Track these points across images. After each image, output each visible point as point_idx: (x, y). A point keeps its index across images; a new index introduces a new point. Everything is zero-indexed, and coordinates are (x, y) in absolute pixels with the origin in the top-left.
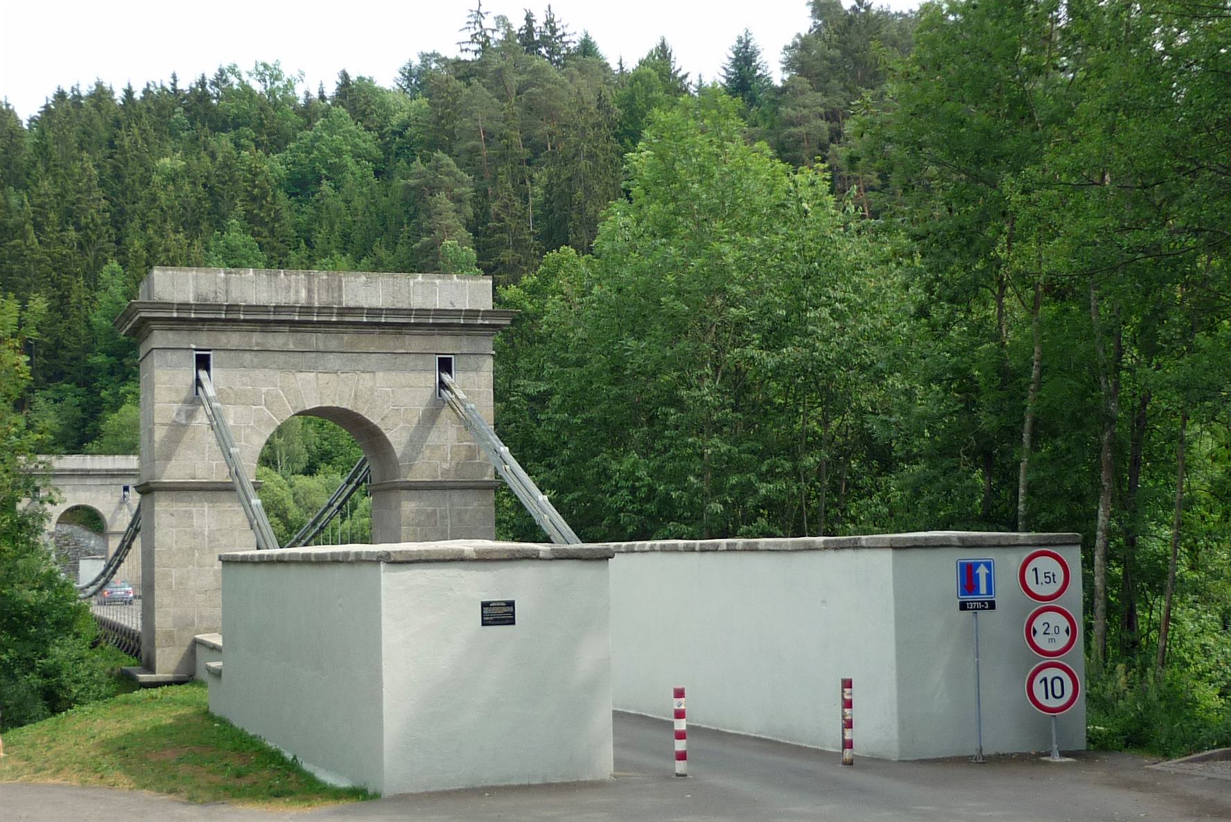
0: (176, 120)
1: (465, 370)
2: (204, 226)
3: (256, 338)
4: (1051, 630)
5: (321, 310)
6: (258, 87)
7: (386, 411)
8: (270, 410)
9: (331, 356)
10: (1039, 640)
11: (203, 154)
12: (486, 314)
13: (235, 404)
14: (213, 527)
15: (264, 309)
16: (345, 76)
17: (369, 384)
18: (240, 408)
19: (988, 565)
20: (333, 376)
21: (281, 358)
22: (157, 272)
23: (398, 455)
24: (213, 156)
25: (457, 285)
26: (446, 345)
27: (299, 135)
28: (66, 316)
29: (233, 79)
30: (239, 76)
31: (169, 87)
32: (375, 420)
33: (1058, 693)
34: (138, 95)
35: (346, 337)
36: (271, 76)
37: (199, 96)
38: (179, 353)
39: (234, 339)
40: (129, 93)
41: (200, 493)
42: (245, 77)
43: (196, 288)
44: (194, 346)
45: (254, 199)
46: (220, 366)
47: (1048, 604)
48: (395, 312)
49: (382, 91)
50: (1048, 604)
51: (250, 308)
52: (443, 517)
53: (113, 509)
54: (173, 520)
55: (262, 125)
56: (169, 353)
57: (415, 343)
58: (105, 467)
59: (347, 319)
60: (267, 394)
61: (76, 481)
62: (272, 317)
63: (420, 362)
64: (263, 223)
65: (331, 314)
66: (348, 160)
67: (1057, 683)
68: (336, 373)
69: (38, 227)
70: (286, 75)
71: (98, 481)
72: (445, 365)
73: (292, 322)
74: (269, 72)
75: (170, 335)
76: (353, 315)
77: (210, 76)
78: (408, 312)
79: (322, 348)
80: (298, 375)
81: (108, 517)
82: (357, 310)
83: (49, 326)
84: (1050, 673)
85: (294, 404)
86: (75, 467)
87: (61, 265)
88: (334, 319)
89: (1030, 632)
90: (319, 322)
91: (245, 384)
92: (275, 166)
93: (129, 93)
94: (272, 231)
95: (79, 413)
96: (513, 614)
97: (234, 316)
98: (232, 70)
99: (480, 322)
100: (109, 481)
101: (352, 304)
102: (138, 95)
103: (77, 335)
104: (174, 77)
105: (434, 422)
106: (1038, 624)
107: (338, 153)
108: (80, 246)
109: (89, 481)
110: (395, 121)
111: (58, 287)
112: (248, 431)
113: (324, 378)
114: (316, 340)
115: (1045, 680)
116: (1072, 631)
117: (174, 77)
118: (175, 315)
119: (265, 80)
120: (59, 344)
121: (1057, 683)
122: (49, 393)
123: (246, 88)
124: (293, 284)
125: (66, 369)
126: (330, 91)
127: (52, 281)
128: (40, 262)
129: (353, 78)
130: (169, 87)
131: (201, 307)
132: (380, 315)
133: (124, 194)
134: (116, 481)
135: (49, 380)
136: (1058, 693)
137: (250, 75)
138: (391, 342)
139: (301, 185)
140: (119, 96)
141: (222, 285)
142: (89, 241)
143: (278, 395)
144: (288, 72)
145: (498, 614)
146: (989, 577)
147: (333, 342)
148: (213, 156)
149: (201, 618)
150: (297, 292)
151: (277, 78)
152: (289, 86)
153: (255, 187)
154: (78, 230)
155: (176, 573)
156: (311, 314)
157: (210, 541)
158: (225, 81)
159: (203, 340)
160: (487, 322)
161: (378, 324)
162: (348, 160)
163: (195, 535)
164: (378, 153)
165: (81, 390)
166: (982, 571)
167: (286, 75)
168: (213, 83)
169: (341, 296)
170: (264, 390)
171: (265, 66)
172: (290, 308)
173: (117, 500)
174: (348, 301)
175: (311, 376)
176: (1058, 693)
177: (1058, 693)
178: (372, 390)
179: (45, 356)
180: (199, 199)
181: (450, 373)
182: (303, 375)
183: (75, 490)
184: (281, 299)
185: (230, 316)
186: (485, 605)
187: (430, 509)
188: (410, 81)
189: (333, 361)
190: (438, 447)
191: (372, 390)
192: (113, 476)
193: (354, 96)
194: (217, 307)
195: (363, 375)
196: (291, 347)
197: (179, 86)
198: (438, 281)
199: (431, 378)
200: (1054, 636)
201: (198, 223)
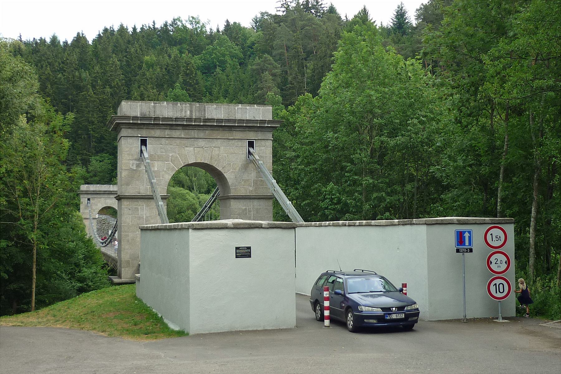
0: (154, 41)
1: (260, 146)
2: (165, 86)
3: (167, 132)
4: (498, 262)
5: (196, 120)
6: (189, 26)
9: (200, 140)
10: (493, 266)
11: (165, 55)
12: (269, 122)
14: (148, 215)
15: (170, 119)
16: (227, 21)
17: (217, 152)
18: (160, 163)
19: (469, 232)
20: (201, 149)
21: (178, 141)
22: (123, 103)
23: (230, 184)
24: (170, 56)
25: (256, 109)
26: (252, 136)
27: (207, 47)
28: (105, 125)
29: (179, 23)
30: (181, 21)
31: (152, 27)
32: (220, 169)
33: (501, 290)
34: (138, 30)
35: (207, 132)
37: (165, 29)
38: (133, 138)
39: (157, 132)
40: (135, 29)
41: (142, 200)
42: (184, 22)
43: (141, 110)
45: (187, 75)
46: (151, 144)
47: (497, 250)
48: (229, 121)
49: (244, 28)
50: (497, 250)
51: (164, 119)
52: (250, 211)
54: (130, 212)
56: (129, 138)
57: (238, 134)
59: (207, 124)
60: (172, 156)
62: (174, 123)
63: (240, 143)
64: (191, 85)
65: (200, 122)
66: (228, 58)
67: (501, 286)
69: (93, 87)
72: (251, 144)
73: (183, 125)
74: (194, 20)
75: (129, 130)
76: (210, 122)
77: (170, 22)
78: (234, 121)
79: (196, 137)
80: (186, 148)
82: (212, 120)
84: (498, 281)
88: (202, 124)
89: (489, 263)
90: (194, 125)
92: (196, 61)
93: (135, 29)
94: (195, 89)
95: (110, 167)
96: (250, 252)
97: (158, 122)
99: (266, 125)
101: (210, 117)
102: (138, 30)
104: (154, 22)
105: (246, 169)
106: (492, 259)
107: (224, 55)
108: (111, 94)
110: (248, 42)
111: (102, 112)
112: (163, 173)
114: (194, 133)
115: (496, 284)
116: (508, 262)
117: (154, 22)
118: (131, 122)
119: (192, 24)
120: (102, 138)
121: (501, 286)
122: (98, 158)
123: (185, 27)
124: (184, 109)
126: (222, 28)
128: (95, 101)
129: (232, 22)
130: (152, 27)
131: (143, 118)
132: (222, 122)
133: (131, 72)
135: (97, 152)
136: (501, 291)
138: (227, 134)
139: (208, 70)
140: (130, 30)
141: (152, 109)
142: (115, 93)
143: (177, 157)
144: (203, 20)
145: (244, 253)
146: (470, 238)
147: (201, 134)
148: (170, 56)
150: (186, 112)
151: (198, 23)
152: (203, 26)
153: (187, 69)
154: (111, 88)
156: (192, 121)
158: (176, 24)
159: (144, 133)
161: (221, 126)
162: (228, 58)
163: (139, 218)
164: (241, 55)
165: (111, 157)
166: (467, 235)
169: (205, 114)
170: (171, 155)
171: (193, 18)
172: (182, 119)
174: (208, 116)
176: (501, 291)
177: (501, 290)
180: (164, 75)
181: (253, 148)
182: (188, 148)
184: (178, 115)
185: (156, 122)
186: (237, 248)
188: (256, 24)
189: (201, 143)
190: (248, 180)
193: (232, 30)
194: (150, 118)
196: (183, 136)
197: (156, 26)
198: (248, 108)
200: (500, 265)
201: (163, 85)
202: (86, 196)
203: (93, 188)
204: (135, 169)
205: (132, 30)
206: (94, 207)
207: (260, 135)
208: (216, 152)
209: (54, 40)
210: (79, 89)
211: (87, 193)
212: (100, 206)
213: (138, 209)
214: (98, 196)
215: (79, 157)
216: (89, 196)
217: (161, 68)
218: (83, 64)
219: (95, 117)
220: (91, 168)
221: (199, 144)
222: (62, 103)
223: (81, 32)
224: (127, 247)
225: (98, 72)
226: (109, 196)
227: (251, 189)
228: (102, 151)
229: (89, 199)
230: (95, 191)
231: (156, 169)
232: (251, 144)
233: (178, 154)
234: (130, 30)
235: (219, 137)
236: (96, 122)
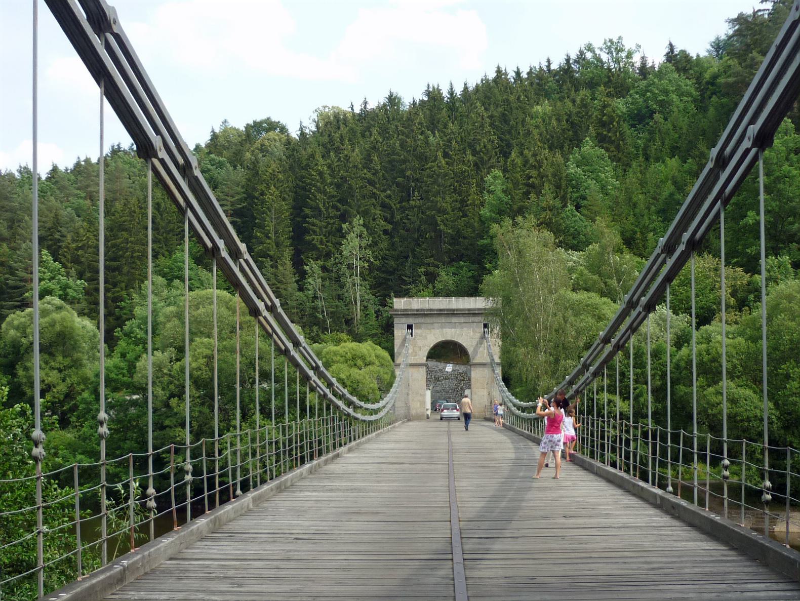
0: (549, 87)
6: (605, 57)
11: (566, 100)
16: (671, 46)
24: (574, 101)
27: (636, 85)
28: (465, 215)
29: (589, 55)
31: (545, 69)
34: (524, 75)
36: (616, 49)
37: (566, 70)
40: (518, 73)
42: (598, 52)
45: (603, 124)
53: (474, 343)
55: (610, 81)
58: (467, 306)
61: (443, 319)
64: (612, 142)
66: (674, 97)
69: (446, 155)
70: (627, 48)
71: (462, 320)
74: (614, 47)
77: (573, 56)
81: (470, 351)
83: (452, 221)
86: (442, 307)
87: (462, 178)
92: (620, 105)
93: (518, 73)
94: (618, 148)
95: (472, 284)
98: (590, 48)
100: (471, 319)
102: (524, 75)
103: (473, 227)
104: (548, 61)
107: (666, 92)
108: (476, 164)
109: (454, 320)
110: (707, 76)
117: (548, 61)
122: (452, 269)
123: (599, 60)
125: (465, 252)
127: (455, 190)
128: (446, 175)
129: (676, 51)
130: (545, 69)
133: (510, 133)
134: (477, 319)
135: (452, 261)
137: (601, 49)
139: (640, 118)
140: (511, 75)
144: (628, 45)
148: (574, 101)
151: (621, 50)
153: (604, 115)
154: (474, 155)
162: (674, 97)
164: (695, 93)
165: (475, 267)
167: (627, 48)
168: (575, 61)
171: (611, 41)
173: (478, 335)
179: (450, 244)
180: (564, 130)
183: (442, 328)
188: (718, 52)
192: (474, 315)
203: (416, 303)
205: (514, 74)
206: (420, 342)
209: (393, 100)
210: (423, 158)
211: (406, 314)
214: (428, 320)
215: (422, 270)
216: (411, 321)
217: (558, 120)
218: (433, 124)
219: (446, 202)
220: (439, 286)
222: (398, 185)
223: (436, 87)
225: (452, 132)
226: (449, 320)
228: (461, 258)
229: (410, 327)
230: (421, 310)
234: (511, 75)
236: (449, 209)
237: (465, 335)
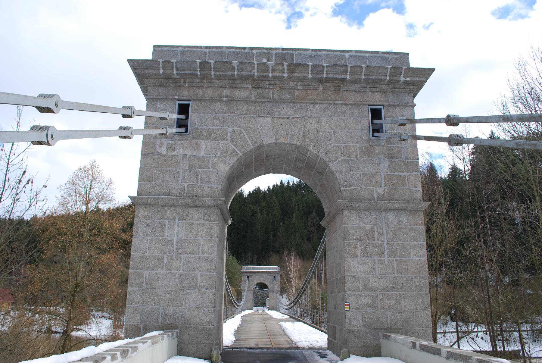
7: (329, 147)
8: (235, 145)
13: (207, 139)
17: (315, 126)
18: (209, 143)
20: (287, 121)
39: (210, 93)
44: (176, 97)
52: (381, 234)
59: (296, 75)
61: (259, 274)
68: (288, 118)
72: (376, 114)
75: (160, 90)
85: (254, 140)
91: (216, 125)
99: (402, 79)
109: (264, 275)
112: (216, 160)
113: (277, 122)
143: (241, 133)
149: (165, 315)
155: (147, 274)
157: (178, 249)
160: (408, 79)
163: (166, 243)
170: (230, 129)
175: (269, 120)
178: (318, 131)
182: (261, 119)
187: (368, 227)
189: (286, 110)
190: (373, 176)
191: (318, 131)
195: (310, 120)
199: (366, 120)
202: (246, 274)
204: (164, 153)
206: (251, 283)
207: (391, 98)
208: (312, 125)
212: (256, 281)
213: (163, 225)
214: (254, 275)
221: (282, 112)
224: (137, 298)
227: (380, 191)
229: (248, 277)
231: (202, 153)
232: (376, 114)
233: (245, 128)
235: (317, 101)
237: (267, 280)
